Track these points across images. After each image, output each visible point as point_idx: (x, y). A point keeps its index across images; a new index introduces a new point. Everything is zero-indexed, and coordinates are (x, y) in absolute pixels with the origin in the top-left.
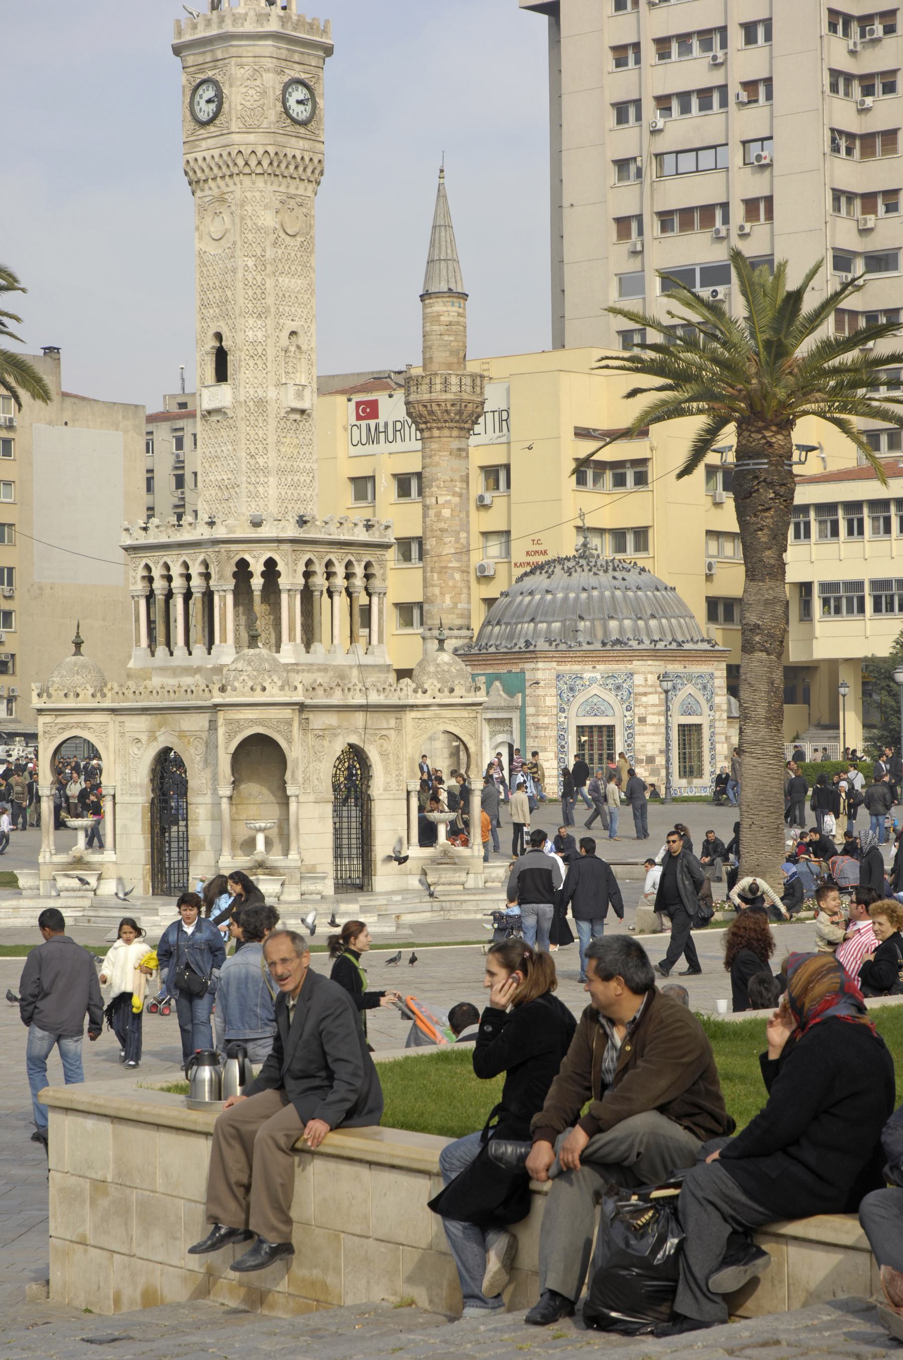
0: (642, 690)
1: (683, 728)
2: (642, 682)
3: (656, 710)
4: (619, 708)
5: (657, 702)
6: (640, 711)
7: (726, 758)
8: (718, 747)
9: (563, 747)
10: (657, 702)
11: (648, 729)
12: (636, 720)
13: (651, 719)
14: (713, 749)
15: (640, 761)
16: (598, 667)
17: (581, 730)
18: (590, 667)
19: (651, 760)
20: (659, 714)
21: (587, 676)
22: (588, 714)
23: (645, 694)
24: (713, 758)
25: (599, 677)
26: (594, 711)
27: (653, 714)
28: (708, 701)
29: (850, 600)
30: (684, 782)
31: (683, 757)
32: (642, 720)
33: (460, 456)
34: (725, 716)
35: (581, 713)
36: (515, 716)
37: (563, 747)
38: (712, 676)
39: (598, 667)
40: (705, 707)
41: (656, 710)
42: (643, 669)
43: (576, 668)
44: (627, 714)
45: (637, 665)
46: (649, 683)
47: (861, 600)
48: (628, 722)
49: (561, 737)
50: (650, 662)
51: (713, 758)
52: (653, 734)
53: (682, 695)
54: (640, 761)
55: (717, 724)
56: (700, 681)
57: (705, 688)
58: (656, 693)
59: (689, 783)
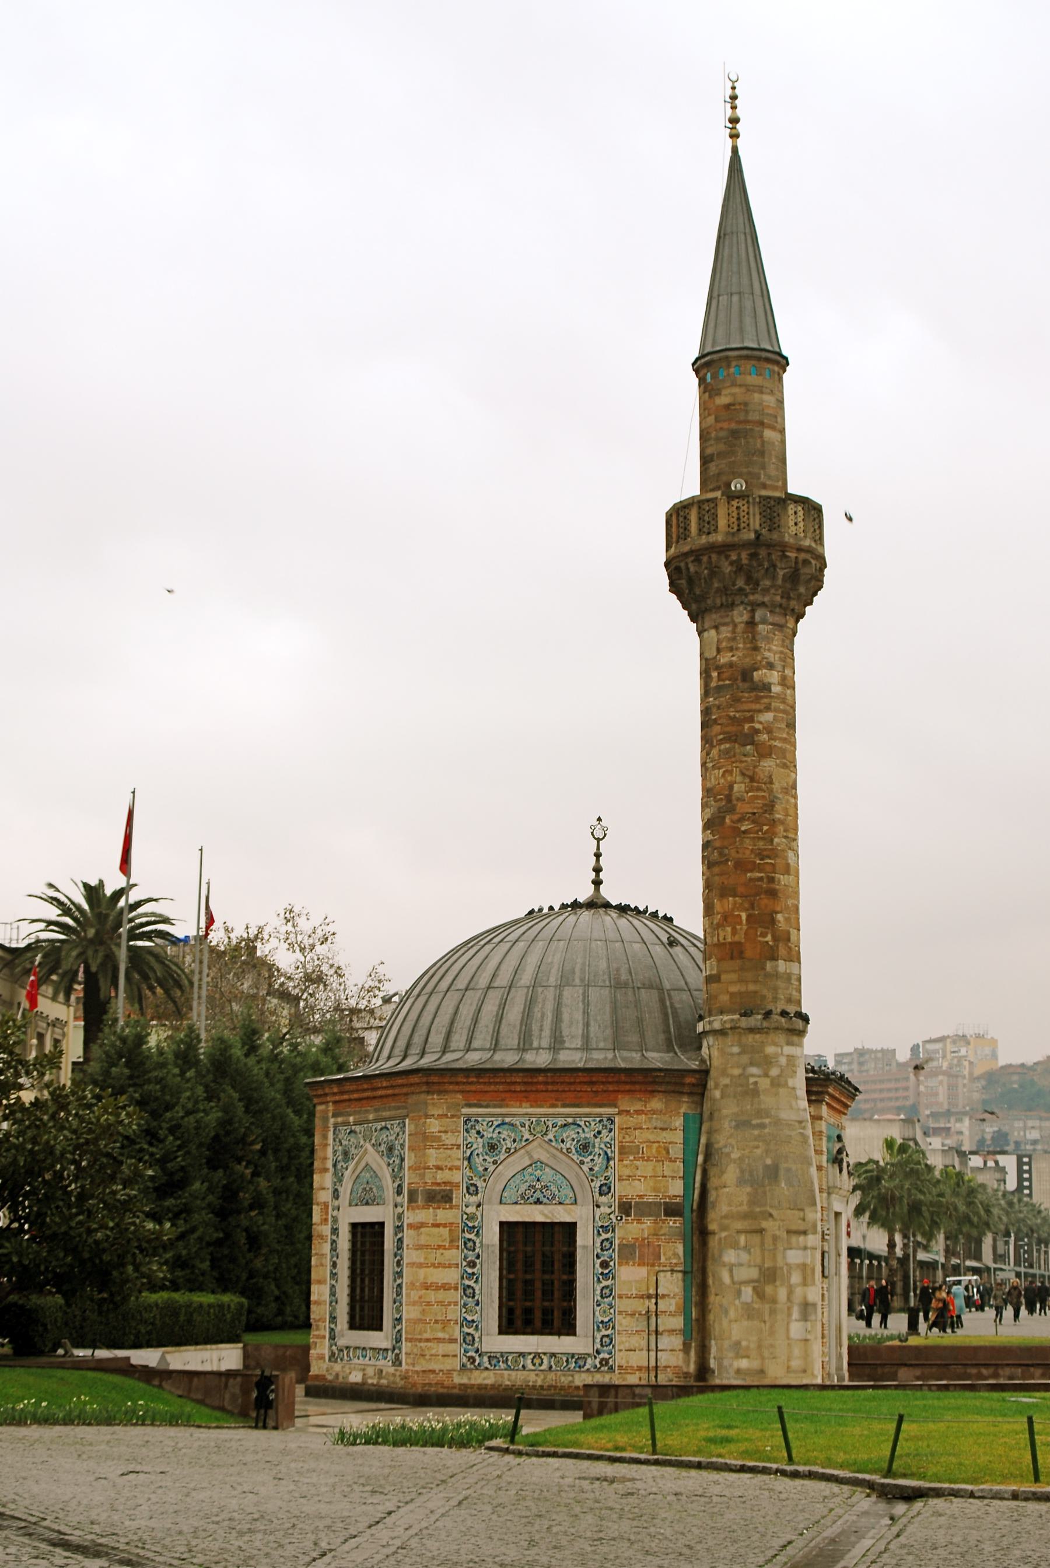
24: (607, 1293)
57: (585, 1148)
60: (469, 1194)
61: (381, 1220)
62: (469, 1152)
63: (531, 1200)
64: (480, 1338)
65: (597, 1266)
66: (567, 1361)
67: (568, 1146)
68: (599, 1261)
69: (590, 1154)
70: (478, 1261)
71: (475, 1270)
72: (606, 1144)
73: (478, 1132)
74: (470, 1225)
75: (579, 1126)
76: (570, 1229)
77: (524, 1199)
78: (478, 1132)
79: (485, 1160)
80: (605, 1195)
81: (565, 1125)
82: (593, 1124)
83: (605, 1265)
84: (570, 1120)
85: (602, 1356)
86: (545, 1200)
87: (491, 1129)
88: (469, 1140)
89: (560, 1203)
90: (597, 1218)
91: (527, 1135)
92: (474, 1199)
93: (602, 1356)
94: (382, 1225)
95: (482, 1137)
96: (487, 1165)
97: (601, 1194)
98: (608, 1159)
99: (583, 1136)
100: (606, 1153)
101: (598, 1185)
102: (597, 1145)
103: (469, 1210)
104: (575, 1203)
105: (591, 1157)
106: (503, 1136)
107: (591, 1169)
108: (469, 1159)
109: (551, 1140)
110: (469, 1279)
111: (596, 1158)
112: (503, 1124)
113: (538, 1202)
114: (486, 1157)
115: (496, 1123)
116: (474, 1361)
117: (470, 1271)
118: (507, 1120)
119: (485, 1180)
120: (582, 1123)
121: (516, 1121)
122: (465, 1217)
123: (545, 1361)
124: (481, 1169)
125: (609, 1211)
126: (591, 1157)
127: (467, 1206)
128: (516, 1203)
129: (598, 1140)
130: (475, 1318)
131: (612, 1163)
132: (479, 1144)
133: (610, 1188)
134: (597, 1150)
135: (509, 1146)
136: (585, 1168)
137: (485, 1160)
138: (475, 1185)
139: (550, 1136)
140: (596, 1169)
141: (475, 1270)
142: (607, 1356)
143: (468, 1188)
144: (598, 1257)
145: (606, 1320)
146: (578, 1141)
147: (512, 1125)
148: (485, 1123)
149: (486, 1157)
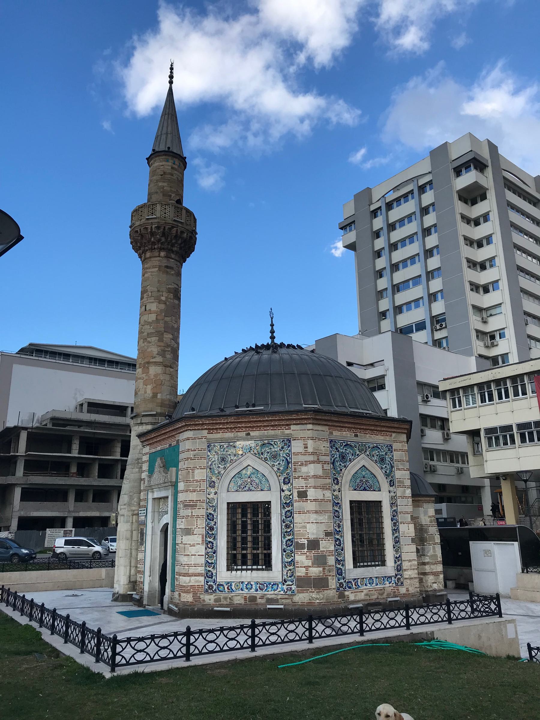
1: (355, 506)
2: (301, 450)
4: (274, 481)
5: (320, 473)
6: (298, 484)
7: (413, 540)
8: (402, 528)
9: (212, 529)
10: (320, 473)
11: (310, 506)
12: (295, 494)
13: (311, 494)
14: (395, 530)
15: (300, 547)
16: (252, 434)
17: (232, 507)
18: (243, 434)
19: (314, 544)
20: (323, 488)
22: (241, 488)
23: (306, 463)
28: (387, 475)
29: (505, 437)
31: (358, 541)
32: (303, 495)
33: (167, 273)
34: (408, 492)
35: (233, 487)
36: (169, 493)
37: (212, 529)
38: (390, 448)
39: (252, 434)
40: (384, 483)
42: (302, 434)
44: (285, 487)
45: (295, 430)
46: (310, 450)
47: (512, 437)
48: (286, 497)
49: (210, 517)
50: (310, 426)
51: (397, 541)
53: (354, 467)
54: (300, 547)
55: (399, 502)
56: (376, 452)
58: (318, 461)
69: (385, 464)
73: (337, 449)
78: (337, 449)
79: (340, 464)
83: (395, 524)
84: (375, 445)
86: (368, 489)
87: (342, 447)
88: (333, 453)
91: (358, 453)
92: (337, 487)
106: (347, 452)
110: (338, 534)
113: (365, 489)
115: (344, 444)
116: (343, 585)
118: (349, 443)
120: (380, 447)
122: (334, 497)
123: (375, 582)
124: (339, 469)
128: (355, 490)
129: (387, 456)
132: (337, 455)
133: (393, 482)
136: (384, 472)
137: (340, 464)
139: (368, 453)
140: (388, 472)
143: (334, 480)
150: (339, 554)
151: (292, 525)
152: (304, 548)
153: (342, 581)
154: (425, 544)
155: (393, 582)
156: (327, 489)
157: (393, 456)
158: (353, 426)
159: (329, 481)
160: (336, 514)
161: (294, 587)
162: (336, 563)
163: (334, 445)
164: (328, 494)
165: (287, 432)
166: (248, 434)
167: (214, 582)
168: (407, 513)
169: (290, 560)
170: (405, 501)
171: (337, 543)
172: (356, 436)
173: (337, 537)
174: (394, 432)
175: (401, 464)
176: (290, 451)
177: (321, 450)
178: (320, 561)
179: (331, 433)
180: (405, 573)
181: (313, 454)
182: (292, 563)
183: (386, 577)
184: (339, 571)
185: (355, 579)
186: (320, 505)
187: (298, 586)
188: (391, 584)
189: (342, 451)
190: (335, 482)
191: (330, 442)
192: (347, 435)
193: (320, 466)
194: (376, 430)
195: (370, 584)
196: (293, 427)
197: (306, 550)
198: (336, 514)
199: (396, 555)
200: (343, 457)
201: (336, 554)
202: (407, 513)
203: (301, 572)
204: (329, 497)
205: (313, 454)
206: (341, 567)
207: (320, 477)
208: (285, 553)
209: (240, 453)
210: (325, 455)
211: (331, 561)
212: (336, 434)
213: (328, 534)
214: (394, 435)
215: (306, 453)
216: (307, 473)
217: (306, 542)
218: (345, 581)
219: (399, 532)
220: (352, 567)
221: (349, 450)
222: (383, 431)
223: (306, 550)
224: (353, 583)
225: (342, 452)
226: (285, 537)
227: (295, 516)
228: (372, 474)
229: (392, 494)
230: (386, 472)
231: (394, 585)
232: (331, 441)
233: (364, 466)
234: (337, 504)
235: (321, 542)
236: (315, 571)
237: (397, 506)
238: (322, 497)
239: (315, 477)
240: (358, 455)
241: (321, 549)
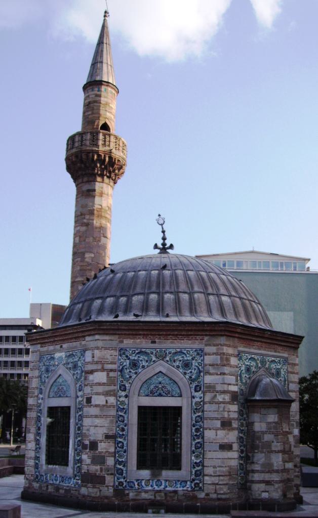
0: (89, 367)
3: (100, 389)
5: (104, 380)
10: (104, 380)
11: (93, 411)
12: (85, 400)
15: (85, 447)
18: (58, 347)
19: (94, 445)
20: (107, 394)
21: (57, 355)
23: (92, 372)
25: (64, 356)
26: (60, 394)
27: (97, 394)
30: (145, 473)
32: (89, 400)
39: (65, 346)
41: (100, 389)
43: (51, 348)
44: (80, 394)
48: (80, 402)
50: (97, 337)
52: (96, 416)
53: (145, 374)
54: (85, 447)
55: (206, 407)
57: (187, 365)
58: (103, 370)
59: (154, 475)
60: (121, 390)
61: (69, 405)
62: (121, 367)
63: (156, 394)
64: (127, 471)
65: (193, 431)
66: (176, 483)
67: (177, 364)
68: (194, 428)
69: (190, 369)
70: (125, 428)
71: (124, 433)
72: (198, 363)
73: (127, 356)
74: (122, 407)
75: (184, 353)
76: (177, 411)
77: (152, 394)
78: (127, 356)
79: (130, 372)
80: (198, 391)
81: (176, 353)
82: (191, 352)
84: (178, 350)
85: (196, 482)
86: (164, 394)
88: (122, 360)
89: (173, 396)
90: (194, 404)
91: (154, 359)
92: (123, 394)
93: (196, 482)
94: (69, 408)
95: (129, 359)
96: (131, 374)
97: (196, 391)
98: (200, 372)
99: (186, 359)
100: (199, 369)
101: (194, 386)
102: (194, 364)
103: (121, 399)
104: (181, 396)
105: (190, 371)
106: (141, 359)
107: (191, 377)
108: (121, 371)
109: (167, 361)
111: (193, 371)
112: (140, 352)
113: (160, 395)
114: (131, 370)
115: (137, 352)
116: (123, 484)
117: (121, 433)
118: (143, 350)
119: (130, 383)
120: (185, 352)
121: (148, 351)
122: (119, 403)
123: (163, 484)
124: (128, 376)
125: (200, 400)
126: (190, 371)
127: (120, 397)
128: (147, 396)
130: (123, 460)
131: (202, 374)
133: (200, 388)
134: (193, 366)
135: (144, 364)
137: (130, 372)
138: (124, 385)
139: (168, 359)
140: (193, 377)
141: (124, 433)
142: (198, 482)
143: (120, 387)
144: (194, 426)
145: (198, 461)
146: (183, 361)
147: (146, 353)
148: (131, 352)
149: (131, 370)
150: (120, 456)
151: (81, 428)
152: (86, 449)
153: (122, 480)
154: (256, 451)
155: (188, 486)
156: (111, 395)
157: (203, 360)
158: (149, 333)
159: (112, 388)
160: (120, 419)
161: (80, 481)
162: (115, 464)
163: (124, 353)
164: (112, 400)
165: (83, 343)
166: (61, 347)
167: (39, 472)
168: (217, 419)
169: (78, 458)
170: (214, 407)
171: (119, 445)
172: (154, 342)
173: (119, 440)
174: (206, 335)
175: (214, 368)
176: (84, 360)
177: (107, 359)
178: (99, 460)
179: (122, 342)
180: (206, 478)
181: (97, 363)
182: (80, 461)
183: (178, 481)
184: (120, 471)
185: (139, 480)
186: (101, 410)
187: (82, 481)
188: (185, 488)
189: (133, 358)
190: (122, 389)
191: (120, 351)
192: (143, 343)
193: (105, 374)
194: (181, 335)
195: (157, 485)
196: (87, 338)
197: (88, 450)
198: (120, 419)
199: (195, 461)
200: (134, 365)
201: (117, 455)
202: (217, 419)
203: (85, 469)
204: (113, 403)
205: (97, 363)
206: (122, 468)
207: (104, 384)
208: (76, 452)
209: (57, 363)
210: (112, 363)
211: (110, 461)
212: (128, 342)
213: (108, 437)
214: (206, 338)
215: (93, 363)
216: (93, 381)
217: (88, 443)
218: (126, 481)
219: (203, 438)
220: (135, 468)
221: (142, 357)
222: (191, 335)
223: (88, 450)
224: (136, 483)
225: (134, 360)
226: (77, 438)
227: (84, 419)
228: (171, 379)
229: (198, 400)
230: (191, 377)
231: (189, 489)
232: (121, 349)
233: (160, 372)
234: (122, 409)
235: (99, 444)
236: (95, 468)
237: (203, 411)
238: (104, 403)
239: (99, 384)
240: (154, 361)
241: (99, 450)
